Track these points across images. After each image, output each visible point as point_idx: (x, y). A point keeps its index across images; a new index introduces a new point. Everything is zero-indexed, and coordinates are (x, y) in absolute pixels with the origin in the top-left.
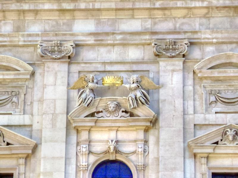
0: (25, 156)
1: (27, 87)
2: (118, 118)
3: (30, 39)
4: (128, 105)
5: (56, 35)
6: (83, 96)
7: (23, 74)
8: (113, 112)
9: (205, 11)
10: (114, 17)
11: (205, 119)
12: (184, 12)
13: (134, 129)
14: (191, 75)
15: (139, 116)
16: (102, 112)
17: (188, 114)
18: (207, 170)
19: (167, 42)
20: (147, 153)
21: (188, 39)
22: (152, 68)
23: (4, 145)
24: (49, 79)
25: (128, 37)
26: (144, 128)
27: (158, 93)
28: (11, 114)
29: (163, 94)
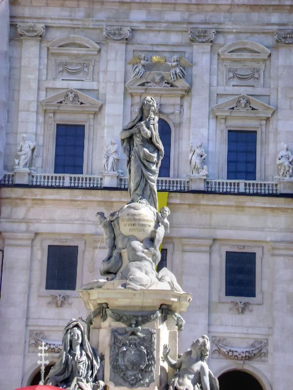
0: (94, 112)
1: (95, 60)
2: (162, 87)
3: (97, 23)
4: (171, 78)
5: (117, 21)
6: (137, 70)
7: (92, 51)
8: (158, 83)
9: (228, 7)
10: (160, 9)
11: (225, 90)
12: (213, 7)
13: (173, 96)
14: (216, 57)
15: (177, 87)
16: (150, 82)
17: (212, 86)
18: (225, 127)
19: (199, 31)
20: (182, 114)
21: (215, 28)
22: (187, 50)
23: (78, 104)
24: (112, 55)
25: (171, 25)
26: (181, 95)
27: (192, 69)
28: (83, 80)
29: (195, 70)
